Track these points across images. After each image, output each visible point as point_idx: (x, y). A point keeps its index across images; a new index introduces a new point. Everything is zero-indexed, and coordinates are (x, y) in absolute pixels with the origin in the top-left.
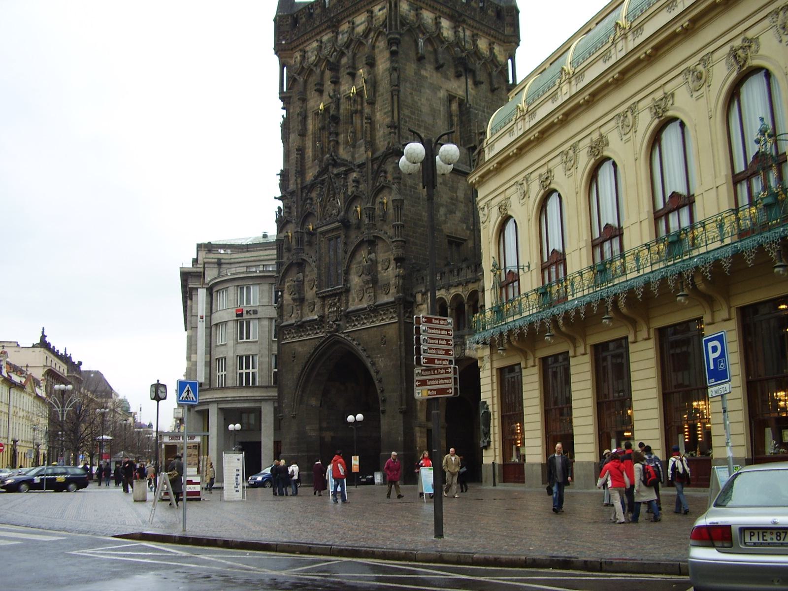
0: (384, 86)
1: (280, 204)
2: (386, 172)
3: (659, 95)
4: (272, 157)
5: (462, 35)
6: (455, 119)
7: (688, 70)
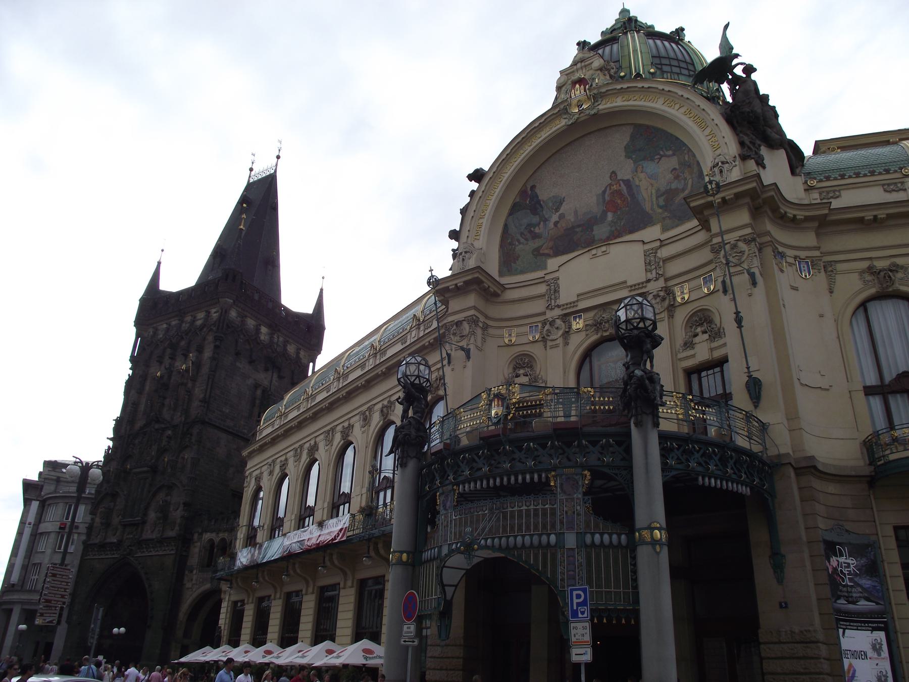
0: (205, 370)
1: (111, 444)
2: (191, 435)
3: (346, 424)
4: (113, 404)
5: (276, 340)
6: (257, 402)
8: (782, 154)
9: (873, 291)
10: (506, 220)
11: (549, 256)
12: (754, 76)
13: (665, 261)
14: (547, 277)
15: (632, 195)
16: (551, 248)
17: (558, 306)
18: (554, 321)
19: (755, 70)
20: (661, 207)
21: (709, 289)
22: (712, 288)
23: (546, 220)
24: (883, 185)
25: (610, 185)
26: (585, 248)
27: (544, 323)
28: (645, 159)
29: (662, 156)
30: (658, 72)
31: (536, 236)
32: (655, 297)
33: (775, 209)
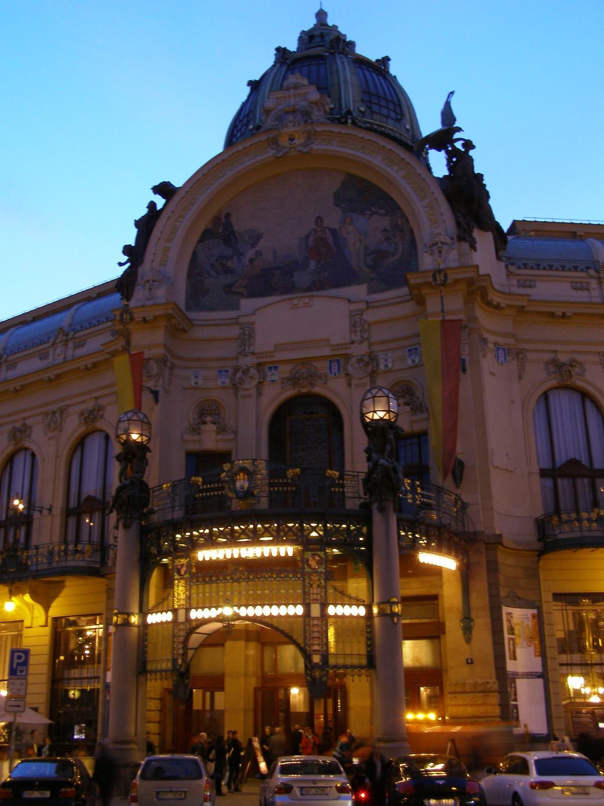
8: (489, 236)
9: (553, 383)
10: (196, 247)
11: (242, 295)
12: (472, 153)
14: (242, 320)
16: (245, 287)
17: (253, 354)
18: (248, 369)
19: (473, 147)
21: (413, 361)
22: (417, 361)
23: (240, 255)
24: (571, 282)
25: (315, 230)
26: (284, 293)
27: (237, 370)
29: (373, 213)
30: (368, 112)
31: (229, 271)
33: (484, 297)
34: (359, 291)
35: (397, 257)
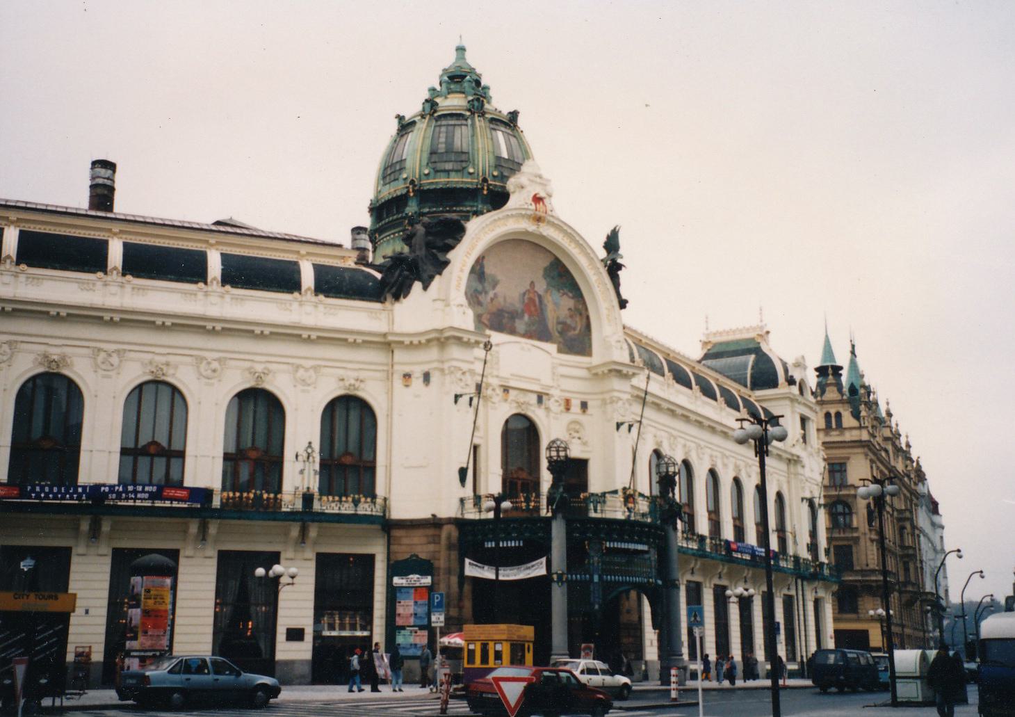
7: (203, 359)
11: (487, 326)
12: (619, 273)
13: (562, 376)
15: (542, 309)
17: (497, 377)
20: (559, 332)
23: (486, 293)
28: (554, 287)
29: (564, 294)
31: (480, 303)
32: (557, 401)
34: (552, 347)
35: (577, 332)
